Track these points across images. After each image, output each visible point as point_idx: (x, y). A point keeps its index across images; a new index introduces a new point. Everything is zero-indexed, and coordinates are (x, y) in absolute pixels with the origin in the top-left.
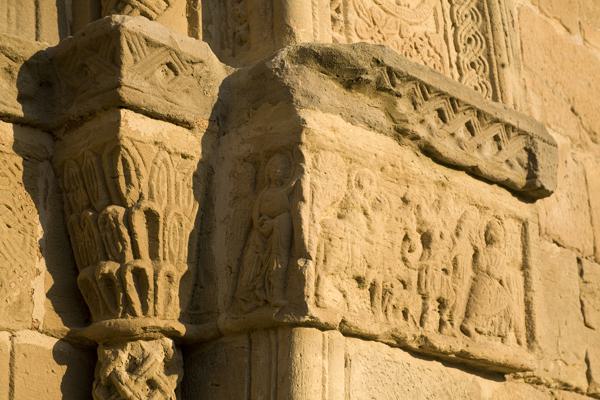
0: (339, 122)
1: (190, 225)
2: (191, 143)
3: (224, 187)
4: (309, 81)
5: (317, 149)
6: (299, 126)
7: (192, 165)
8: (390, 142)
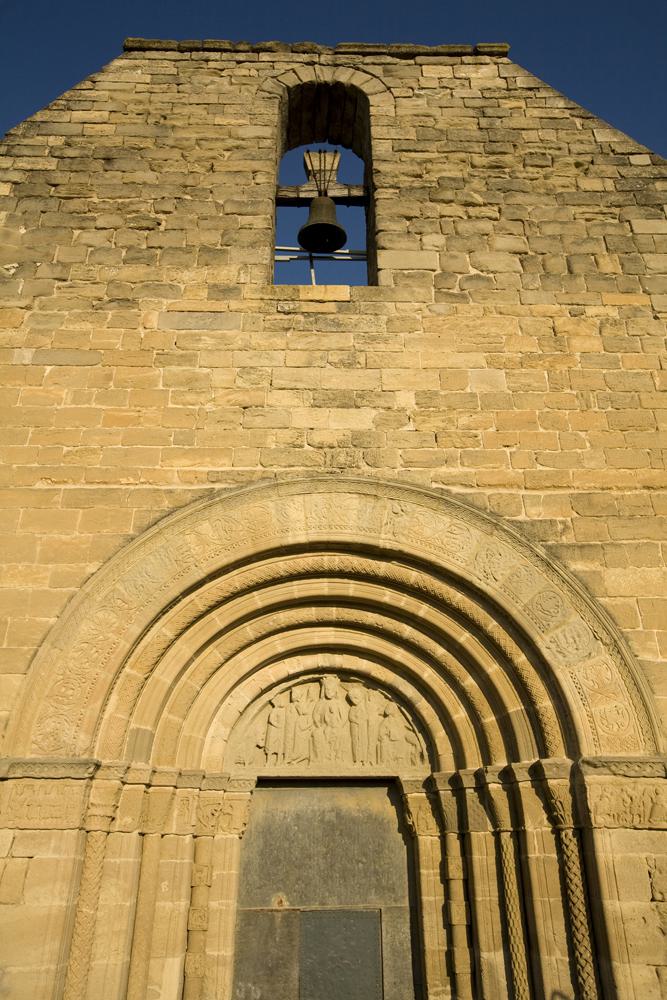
0: (595, 776)
1: (570, 802)
2: (567, 782)
3: (577, 792)
4: (585, 768)
5: (590, 785)
6: (584, 781)
7: (568, 787)
8: (613, 776)
